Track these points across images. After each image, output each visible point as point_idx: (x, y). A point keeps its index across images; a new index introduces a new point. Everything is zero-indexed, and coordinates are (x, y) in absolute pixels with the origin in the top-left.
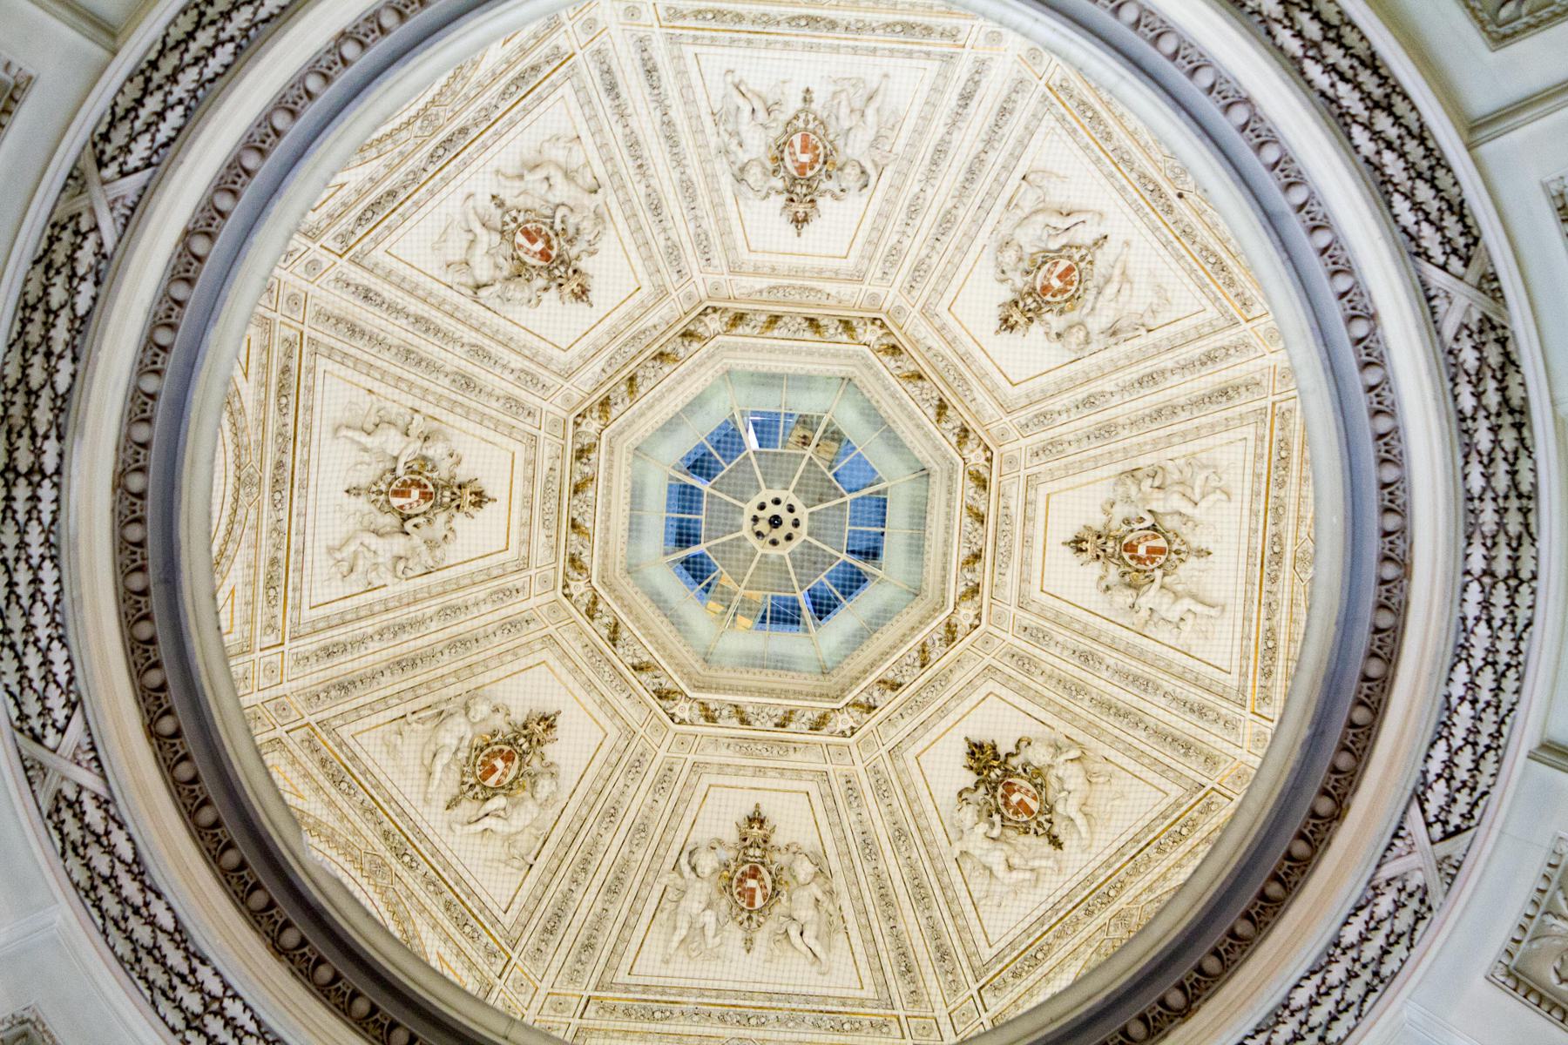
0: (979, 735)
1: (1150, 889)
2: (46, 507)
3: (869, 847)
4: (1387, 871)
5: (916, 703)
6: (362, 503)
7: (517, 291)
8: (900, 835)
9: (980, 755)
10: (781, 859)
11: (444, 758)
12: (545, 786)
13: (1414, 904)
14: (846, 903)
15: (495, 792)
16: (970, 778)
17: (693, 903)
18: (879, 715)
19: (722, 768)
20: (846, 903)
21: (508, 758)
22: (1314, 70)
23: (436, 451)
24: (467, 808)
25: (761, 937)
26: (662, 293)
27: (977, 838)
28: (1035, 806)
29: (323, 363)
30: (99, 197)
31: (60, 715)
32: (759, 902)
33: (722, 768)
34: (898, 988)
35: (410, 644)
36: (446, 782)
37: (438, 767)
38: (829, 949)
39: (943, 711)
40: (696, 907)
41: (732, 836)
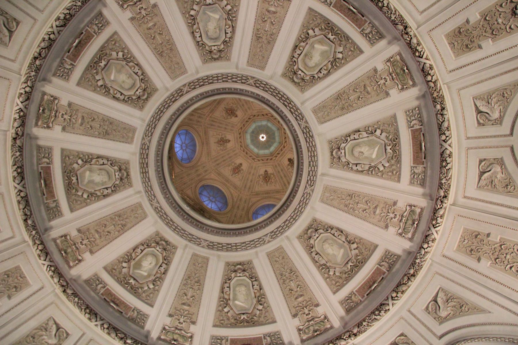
2: (147, 176)
3: (279, 172)
4: (305, 192)
5: (282, 155)
6: (216, 144)
7: (229, 117)
8: (282, 170)
12: (242, 171)
13: (309, 195)
14: (277, 179)
15: (236, 173)
16: (289, 163)
18: (278, 157)
20: (277, 179)
21: (237, 169)
22: (281, 101)
23: (223, 136)
24: (234, 176)
25: (268, 184)
26: (245, 114)
29: (209, 129)
30: (146, 140)
31: (153, 198)
33: (261, 166)
35: (225, 158)
39: (285, 155)
40: (260, 182)
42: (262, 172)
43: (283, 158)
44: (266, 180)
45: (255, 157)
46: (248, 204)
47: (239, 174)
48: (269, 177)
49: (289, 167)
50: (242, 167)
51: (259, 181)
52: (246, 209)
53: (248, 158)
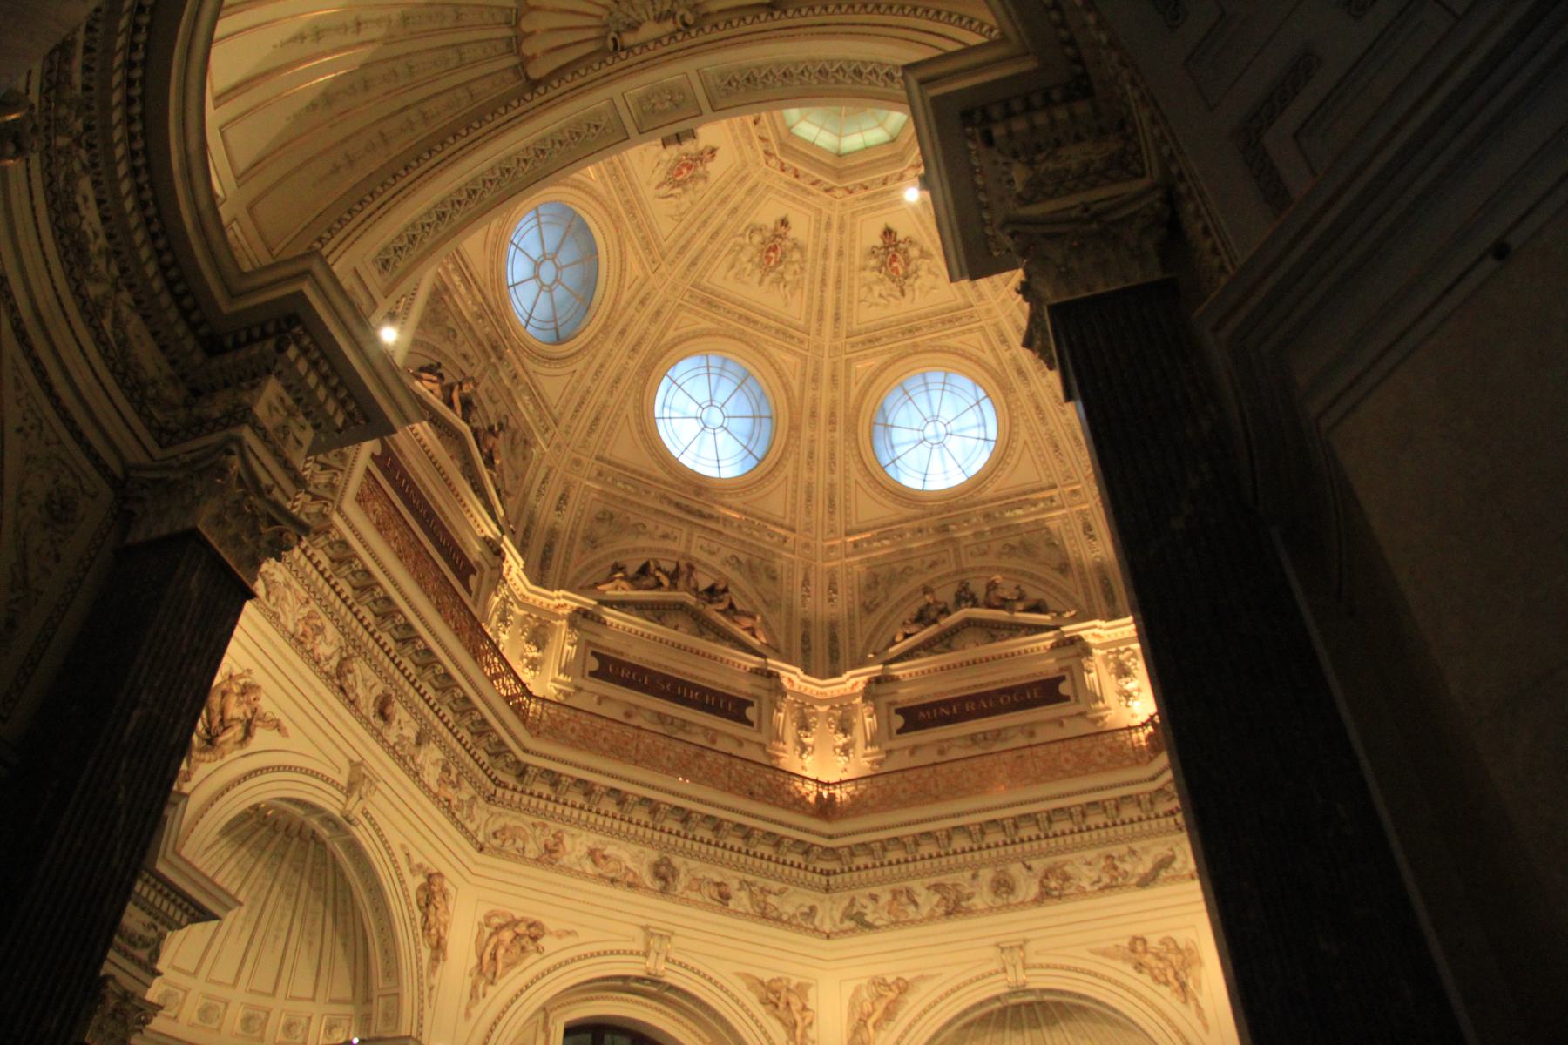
0: (893, 226)
1: (931, 340)
3: (826, 253)
5: (873, 197)
8: (840, 253)
9: (888, 232)
10: (788, 244)
11: (661, 167)
12: (701, 184)
14: (807, 276)
16: (879, 243)
17: (744, 258)
19: (778, 192)
20: (807, 276)
21: (689, 168)
24: (665, 190)
25: (767, 280)
27: (872, 276)
28: (901, 271)
32: (772, 263)
34: (814, 325)
36: (660, 175)
37: (657, 171)
38: (792, 294)
40: (744, 258)
41: (771, 226)
42: (767, 215)
43: (872, 209)
44: (769, 259)
45: (776, 151)
46: (663, 334)
47: (685, 191)
48: (783, 254)
49: (873, 262)
50: (710, 166)
51: (742, 247)
52: (646, 348)
53: (750, 139)
